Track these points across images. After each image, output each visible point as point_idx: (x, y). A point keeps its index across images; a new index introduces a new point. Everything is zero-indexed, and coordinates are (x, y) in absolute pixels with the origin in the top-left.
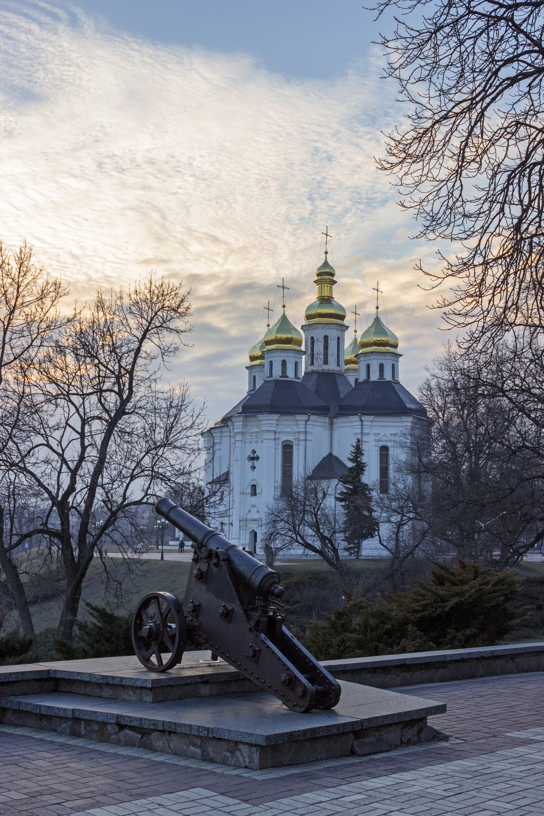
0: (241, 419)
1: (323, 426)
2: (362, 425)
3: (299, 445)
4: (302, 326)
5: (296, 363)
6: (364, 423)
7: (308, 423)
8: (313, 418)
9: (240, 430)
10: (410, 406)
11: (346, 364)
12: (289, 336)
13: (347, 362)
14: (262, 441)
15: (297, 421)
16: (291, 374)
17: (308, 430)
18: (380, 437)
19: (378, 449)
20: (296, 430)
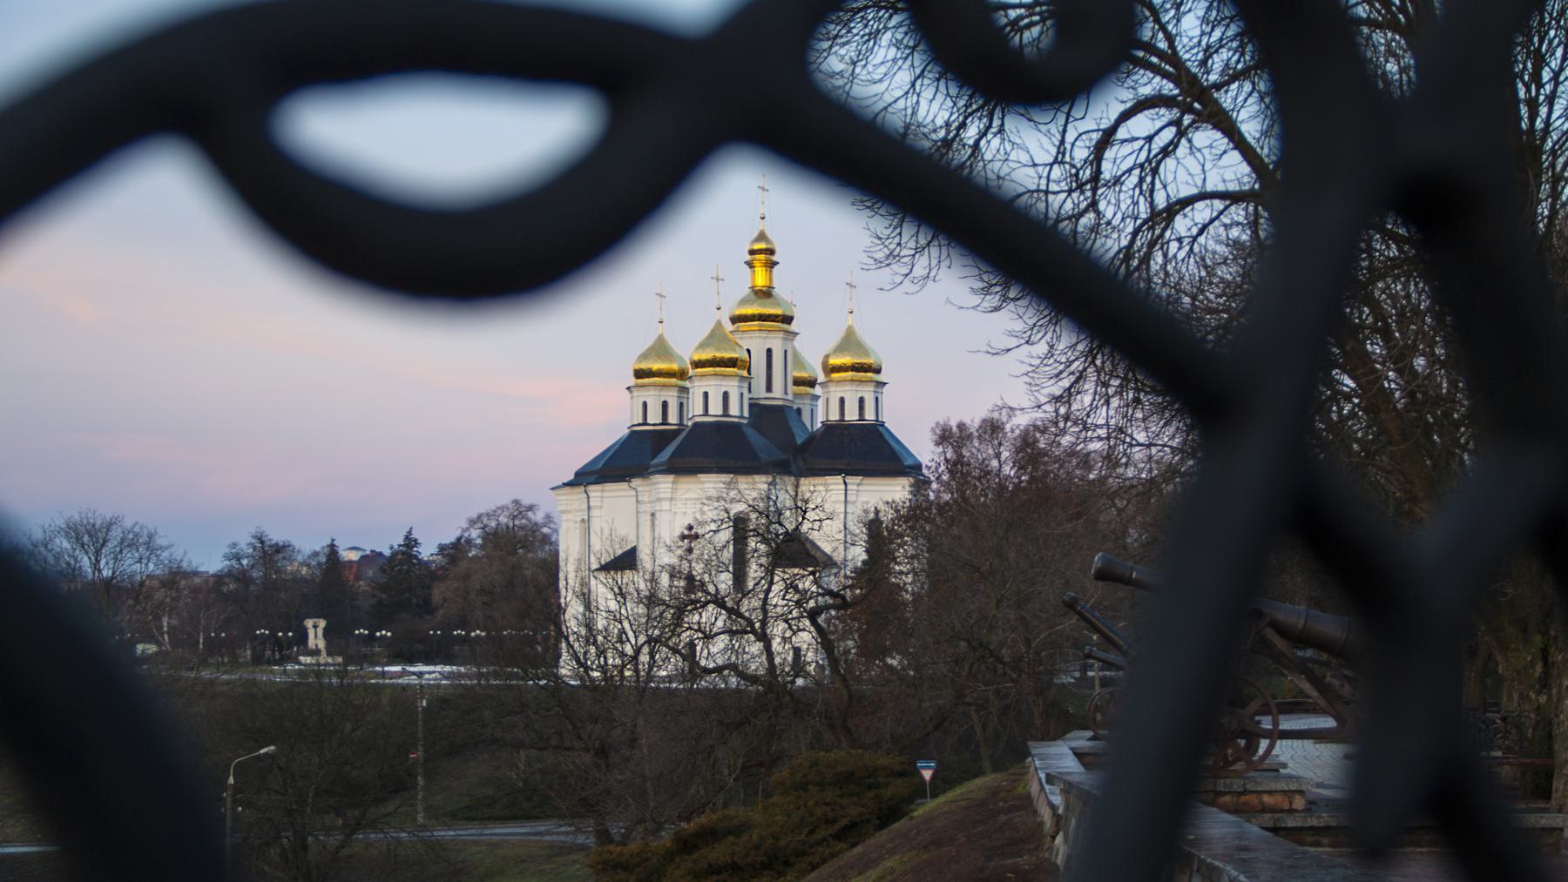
2: (846, 490)
6: (849, 487)
9: (669, 495)
12: (734, 355)
16: (734, 410)
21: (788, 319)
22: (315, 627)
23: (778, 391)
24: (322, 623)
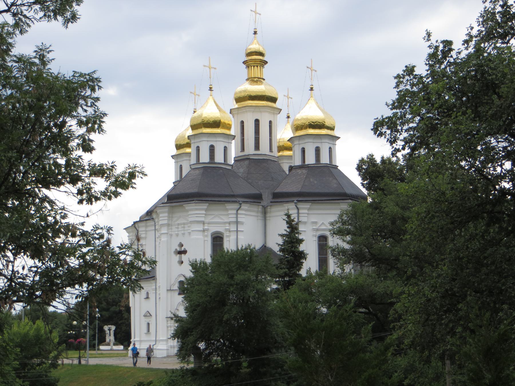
0: (166, 209)
1: (257, 216)
2: (298, 213)
3: (228, 236)
4: (231, 110)
5: (225, 149)
6: (301, 211)
7: (239, 212)
8: (245, 206)
9: (166, 222)
10: (349, 191)
11: (279, 151)
13: (281, 148)
14: (190, 233)
15: (227, 210)
17: (239, 220)
18: (318, 225)
19: (316, 239)
20: (226, 220)
21: (274, 100)
22: (110, 330)
23: (264, 148)
24: (113, 328)
